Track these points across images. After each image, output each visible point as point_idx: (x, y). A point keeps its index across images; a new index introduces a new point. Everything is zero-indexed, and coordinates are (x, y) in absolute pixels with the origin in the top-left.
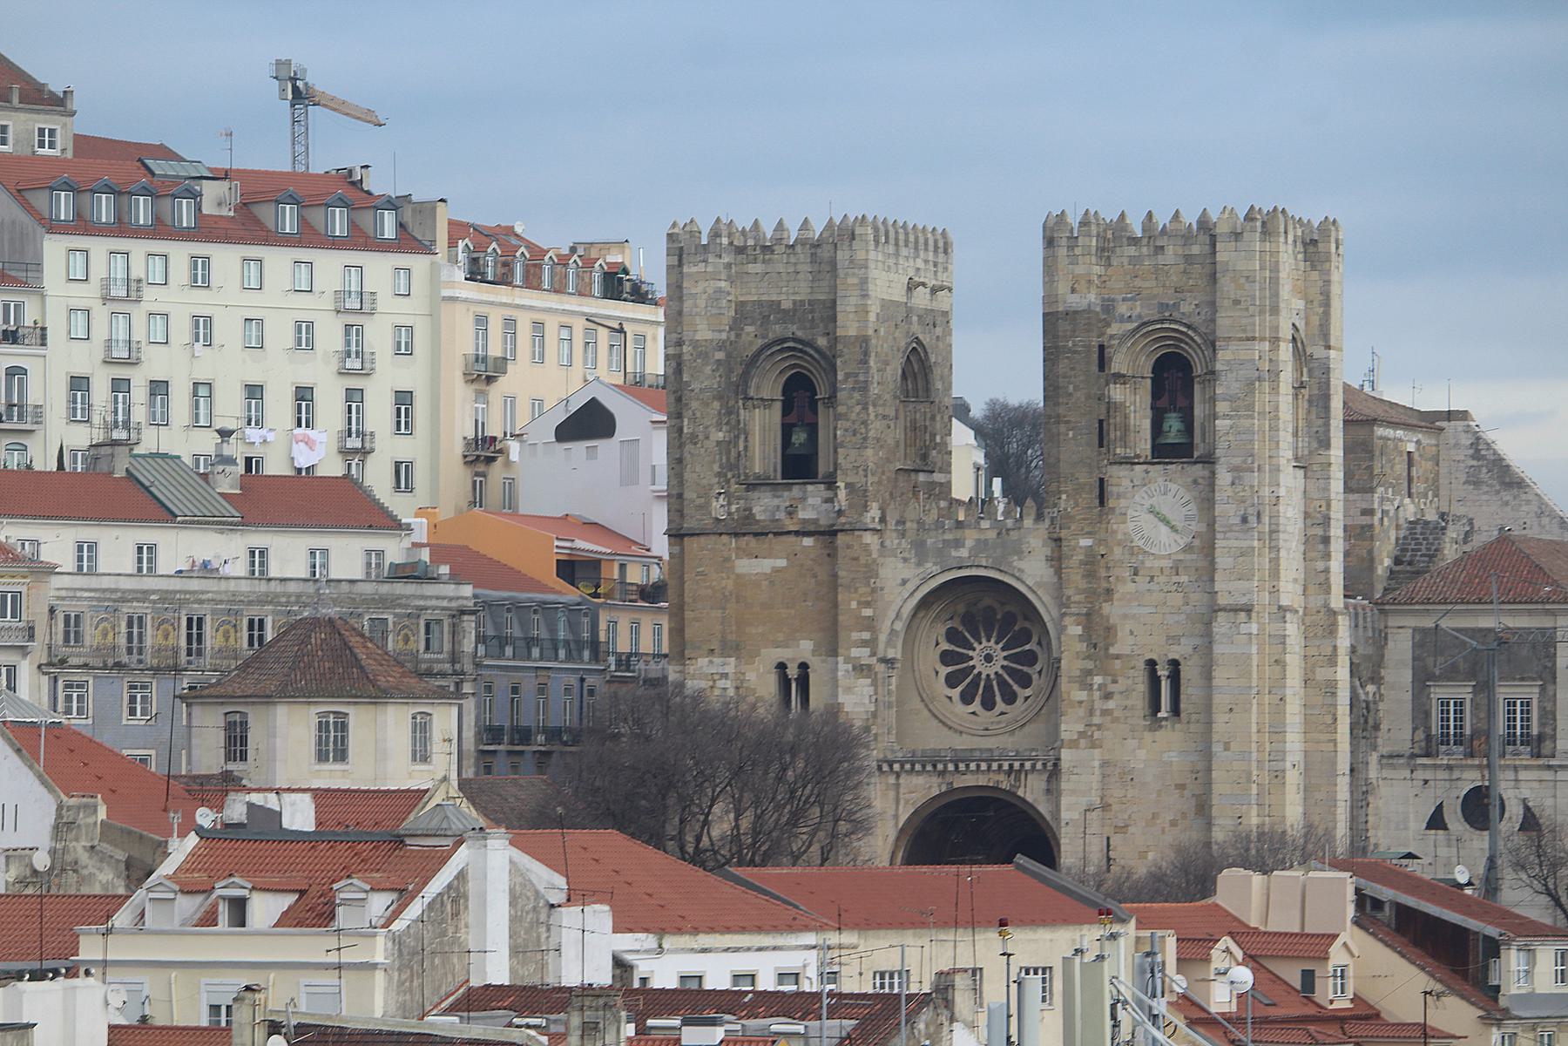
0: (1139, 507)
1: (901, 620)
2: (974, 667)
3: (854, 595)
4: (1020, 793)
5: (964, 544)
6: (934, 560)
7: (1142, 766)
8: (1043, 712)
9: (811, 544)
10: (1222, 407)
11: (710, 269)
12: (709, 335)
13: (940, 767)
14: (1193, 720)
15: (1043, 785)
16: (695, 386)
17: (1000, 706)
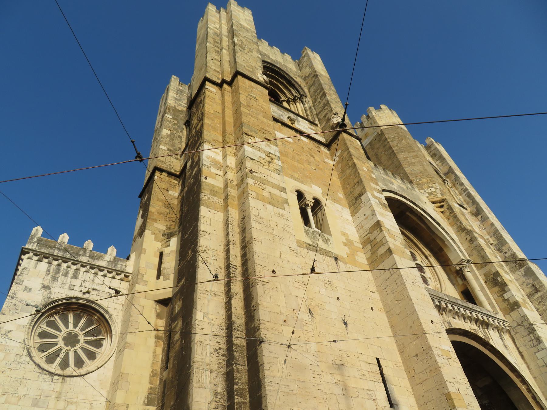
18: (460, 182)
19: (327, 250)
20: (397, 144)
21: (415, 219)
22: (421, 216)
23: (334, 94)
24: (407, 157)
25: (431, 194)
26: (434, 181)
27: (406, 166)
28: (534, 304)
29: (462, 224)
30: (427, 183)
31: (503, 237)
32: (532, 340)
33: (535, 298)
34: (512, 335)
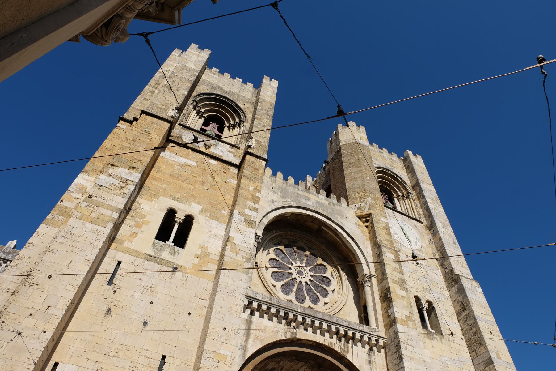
0: (394, 225)
1: (268, 219)
2: (291, 274)
3: (252, 184)
4: (349, 357)
5: (310, 199)
6: (292, 199)
7: (430, 361)
8: (341, 313)
9: (215, 164)
10: (427, 199)
11: (201, 55)
12: (194, 68)
13: (291, 316)
14: (451, 340)
15: (366, 356)
16: (179, 75)
17: (308, 303)
18: (422, 195)
19: (170, 260)
20: (348, 159)
21: (330, 233)
22: (335, 230)
23: (267, 118)
24: (352, 172)
25: (359, 208)
26: (367, 196)
27: (348, 181)
28: (461, 323)
29: (377, 239)
30: (361, 198)
31: (446, 252)
32: (397, 358)
33: (462, 316)
34: (387, 351)
